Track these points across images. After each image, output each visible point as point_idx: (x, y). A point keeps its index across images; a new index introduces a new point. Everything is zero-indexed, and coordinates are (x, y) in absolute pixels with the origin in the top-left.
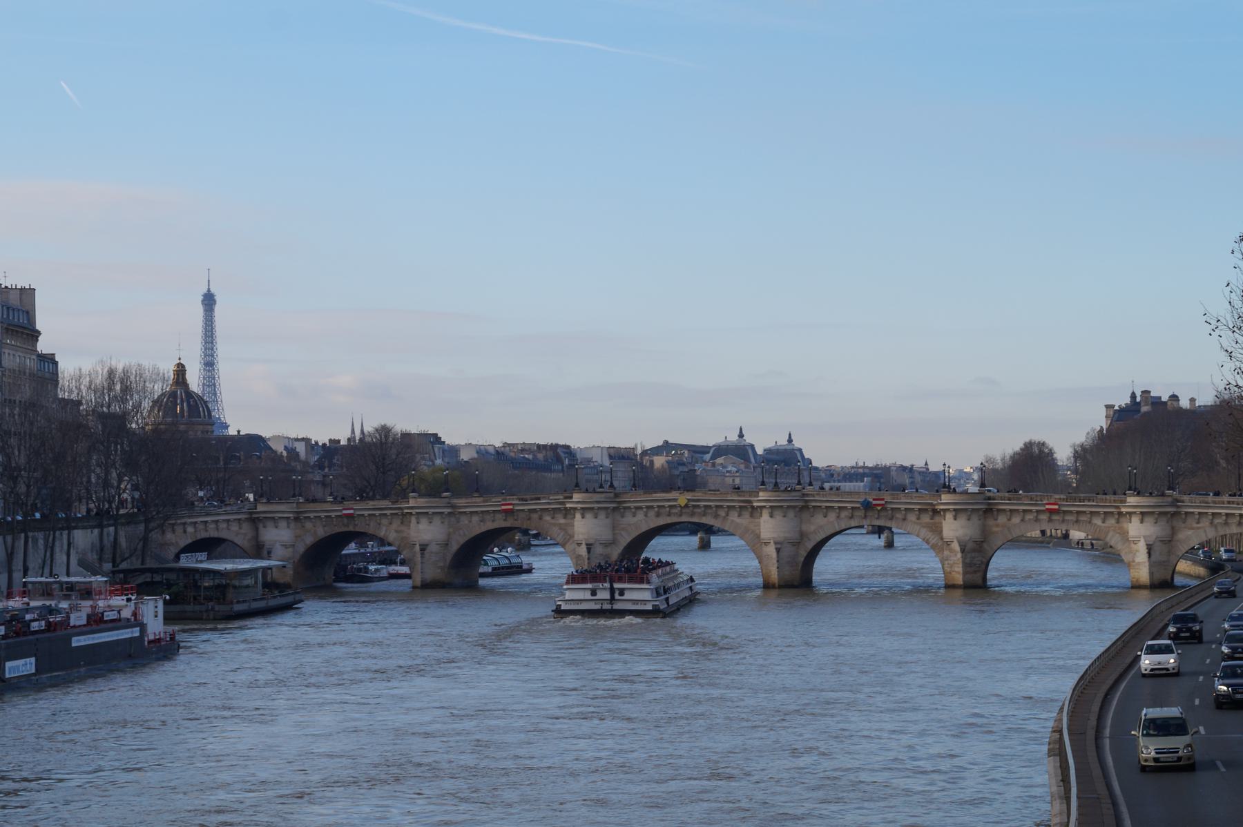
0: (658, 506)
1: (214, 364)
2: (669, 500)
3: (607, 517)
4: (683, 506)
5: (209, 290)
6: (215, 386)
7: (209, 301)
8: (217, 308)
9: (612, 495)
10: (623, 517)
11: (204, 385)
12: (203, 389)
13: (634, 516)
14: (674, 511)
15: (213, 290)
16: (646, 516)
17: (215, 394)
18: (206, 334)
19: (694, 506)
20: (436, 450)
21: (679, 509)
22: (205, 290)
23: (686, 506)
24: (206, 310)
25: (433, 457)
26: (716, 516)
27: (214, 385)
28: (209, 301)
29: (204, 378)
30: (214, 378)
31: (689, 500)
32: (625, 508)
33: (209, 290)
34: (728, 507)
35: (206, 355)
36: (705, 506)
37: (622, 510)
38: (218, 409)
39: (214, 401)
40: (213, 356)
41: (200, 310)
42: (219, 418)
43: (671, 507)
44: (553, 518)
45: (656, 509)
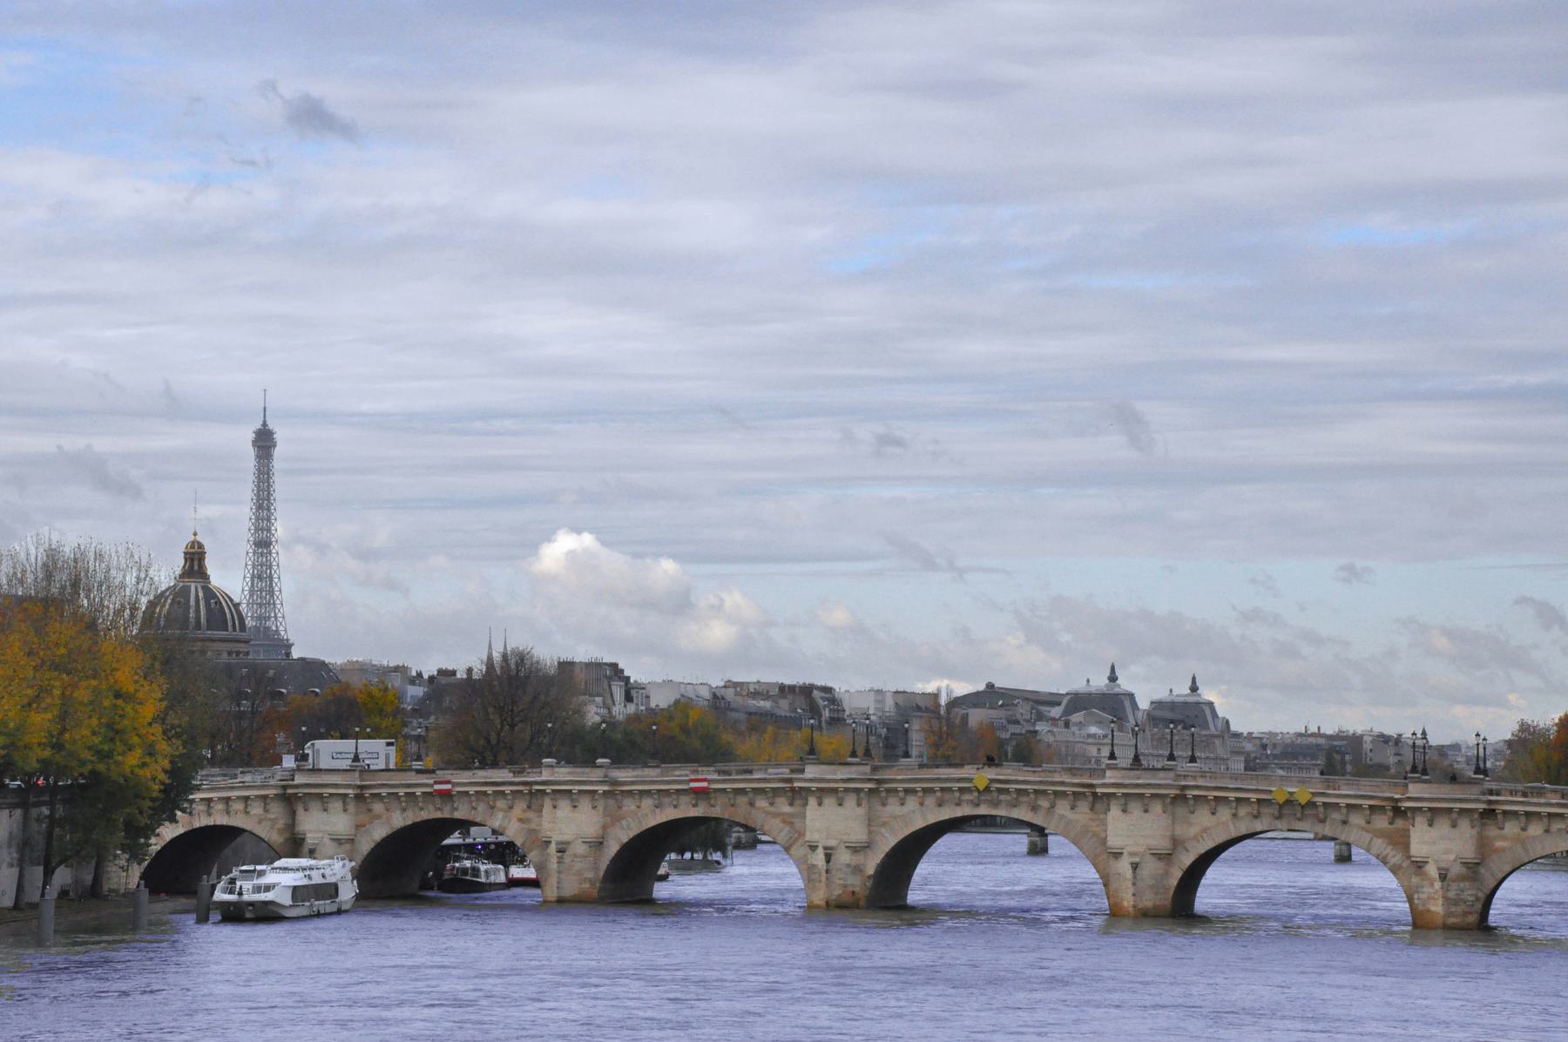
0: (942, 789)
1: (271, 543)
2: (959, 780)
3: (859, 805)
4: (981, 789)
5: (265, 424)
7: (264, 441)
8: (278, 452)
9: (867, 769)
10: (884, 805)
13: (902, 804)
14: (967, 797)
16: (922, 804)
17: (271, 593)
19: (1000, 791)
20: (614, 688)
21: (976, 794)
22: (258, 425)
23: (987, 789)
24: (259, 457)
25: (610, 701)
26: (1034, 808)
27: (271, 577)
28: (264, 441)
30: (270, 567)
31: (992, 781)
32: (888, 791)
33: (265, 424)
34: (1055, 793)
35: (257, 530)
36: (1019, 791)
37: (884, 794)
38: (276, 617)
39: (269, 603)
40: (269, 530)
41: (250, 452)
42: (277, 630)
43: (961, 790)
45: (939, 794)
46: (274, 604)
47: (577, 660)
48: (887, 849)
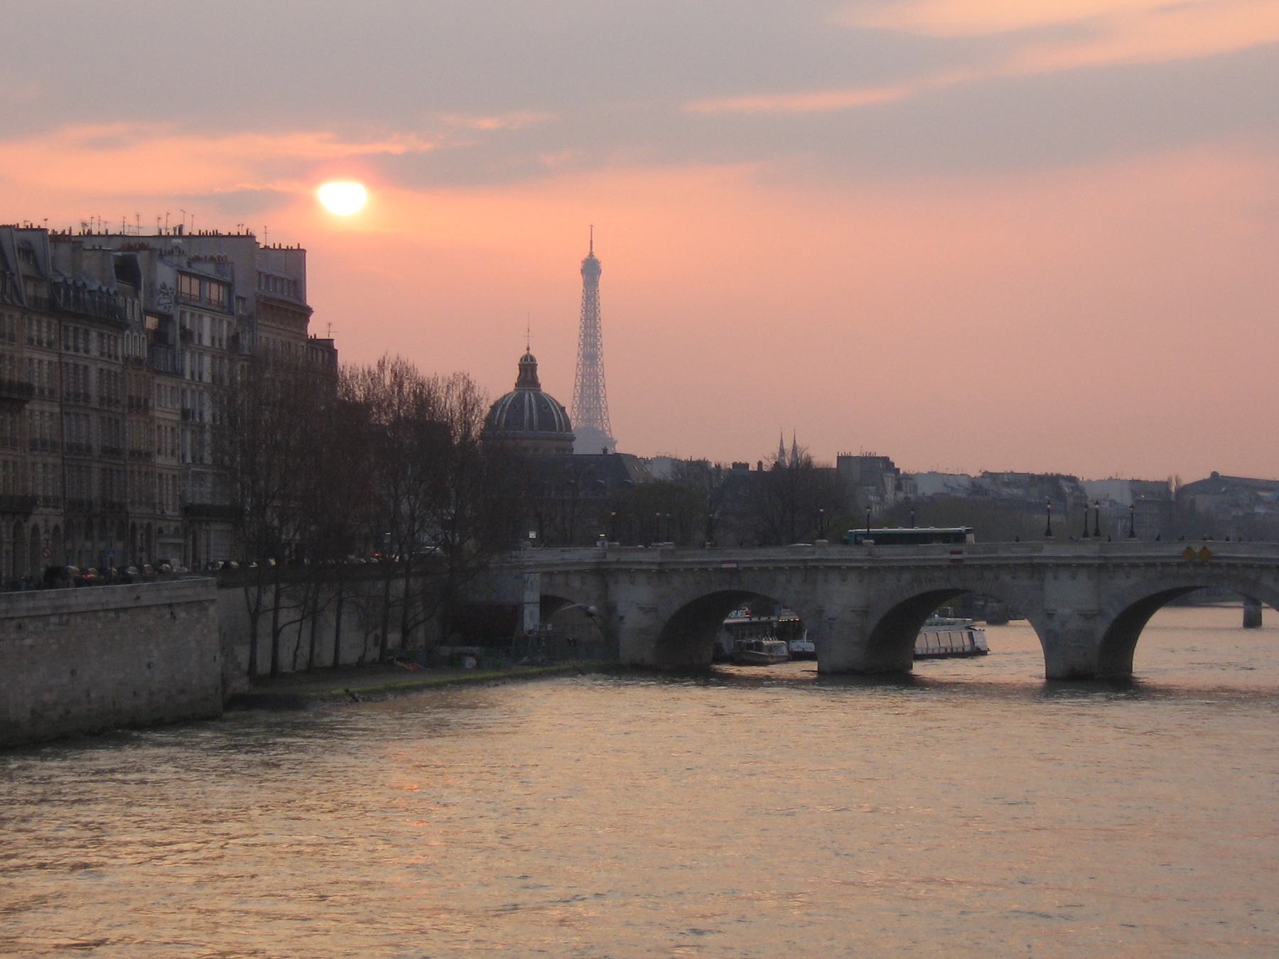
0: (1163, 565)
1: (597, 356)
5: (591, 254)
6: (598, 389)
7: (591, 269)
8: (603, 280)
11: (583, 385)
12: (582, 391)
13: (1128, 577)
15: (597, 255)
17: (598, 398)
18: (586, 315)
22: (586, 255)
24: (586, 284)
27: (597, 385)
28: (591, 269)
29: (583, 376)
30: (597, 377)
33: (591, 254)
39: (596, 408)
41: (578, 281)
42: (603, 431)
44: (1014, 578)
45: (1159, 568)
46: (600, 408)
47: (854, 454)
48: (1114, 616)
